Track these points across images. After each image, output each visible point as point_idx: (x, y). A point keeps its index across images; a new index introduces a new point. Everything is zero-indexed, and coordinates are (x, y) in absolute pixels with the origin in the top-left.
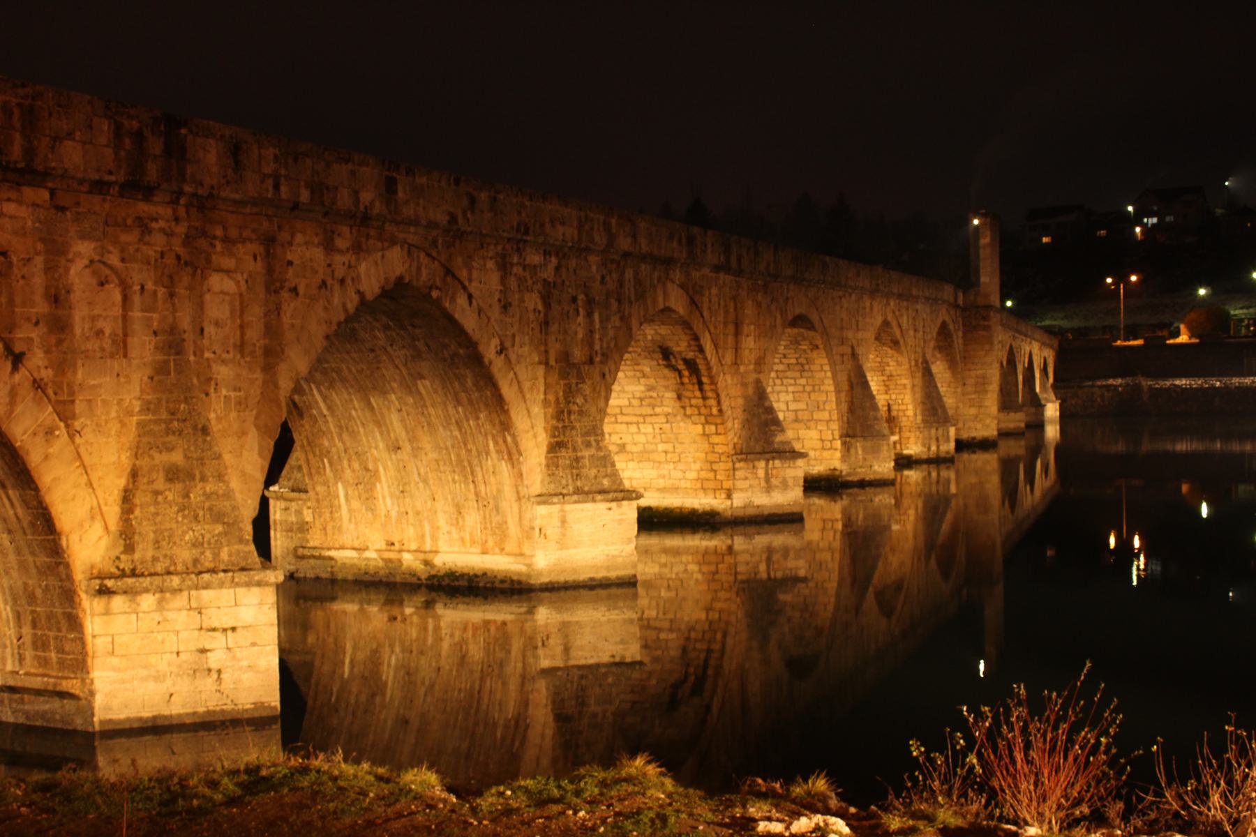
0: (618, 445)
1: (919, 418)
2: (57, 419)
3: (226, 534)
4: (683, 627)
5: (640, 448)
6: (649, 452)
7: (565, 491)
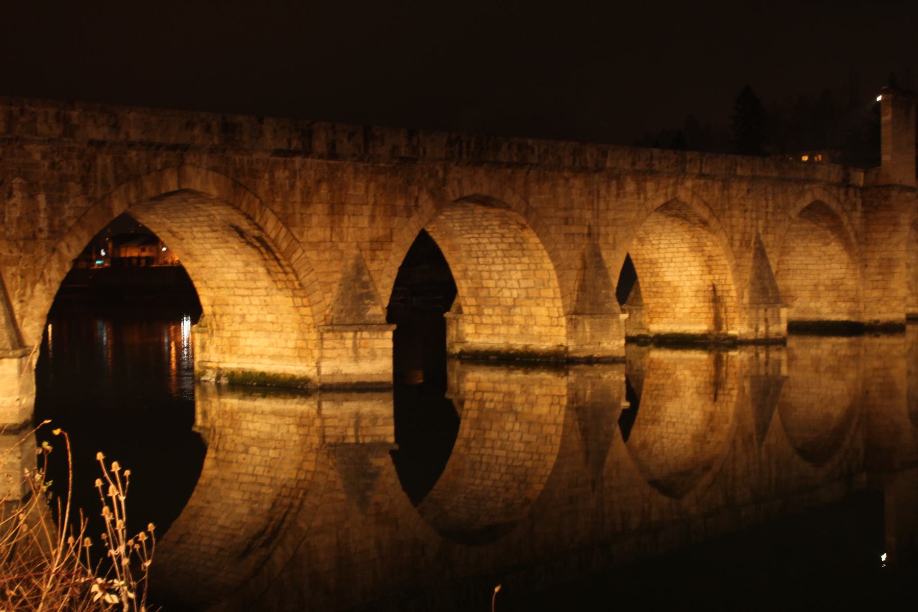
1: (746, 300)
4: (279, 483)
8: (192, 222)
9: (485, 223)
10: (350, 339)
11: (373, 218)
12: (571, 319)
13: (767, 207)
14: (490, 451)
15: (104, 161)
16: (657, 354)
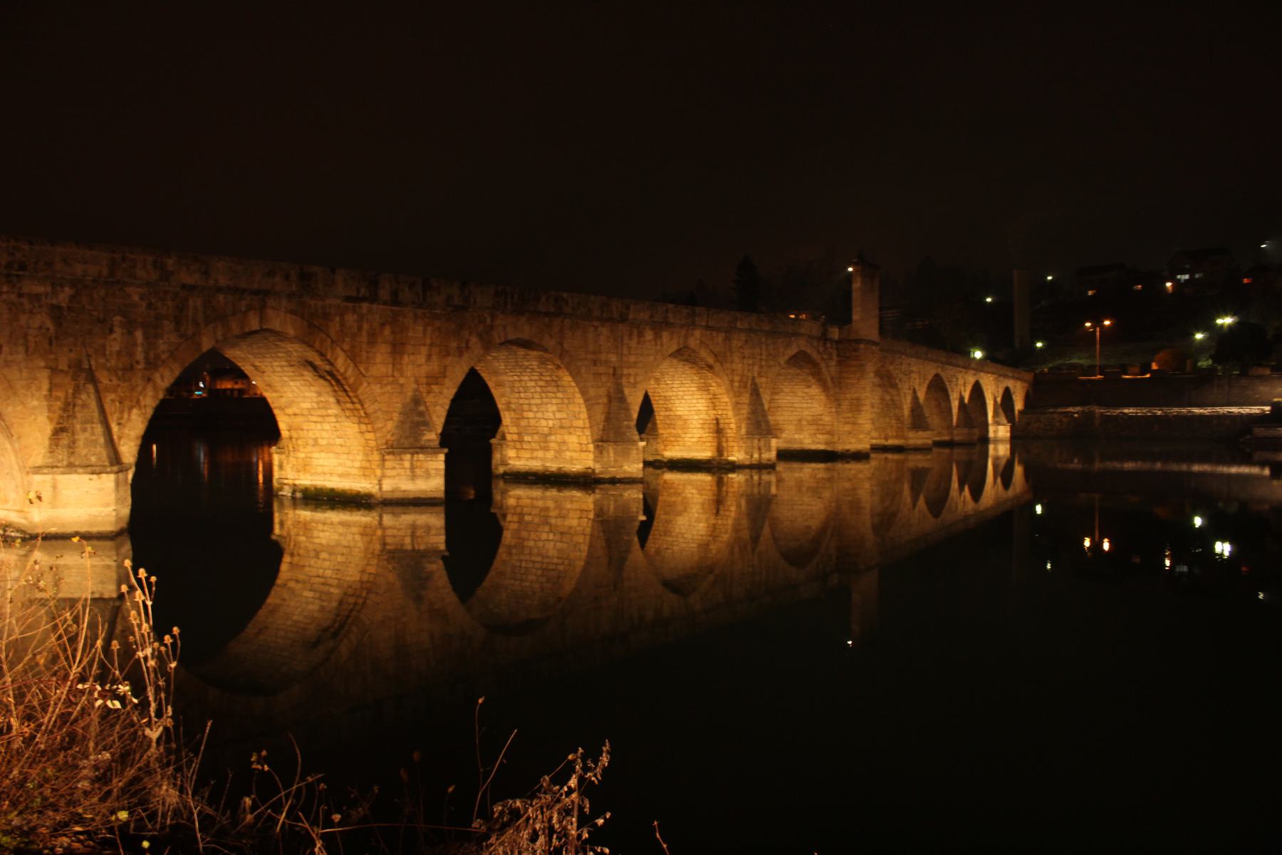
0: (313, 439)
1: (743, 431)
6: (332, 445)
8: (272, 357)
9: (526, 364)
10: (407, 460)
11: (429, 357)
12: (598, 446)
13: (761, 355)
14: (527, 557)
15: (195, 303)
16: (669, 476)
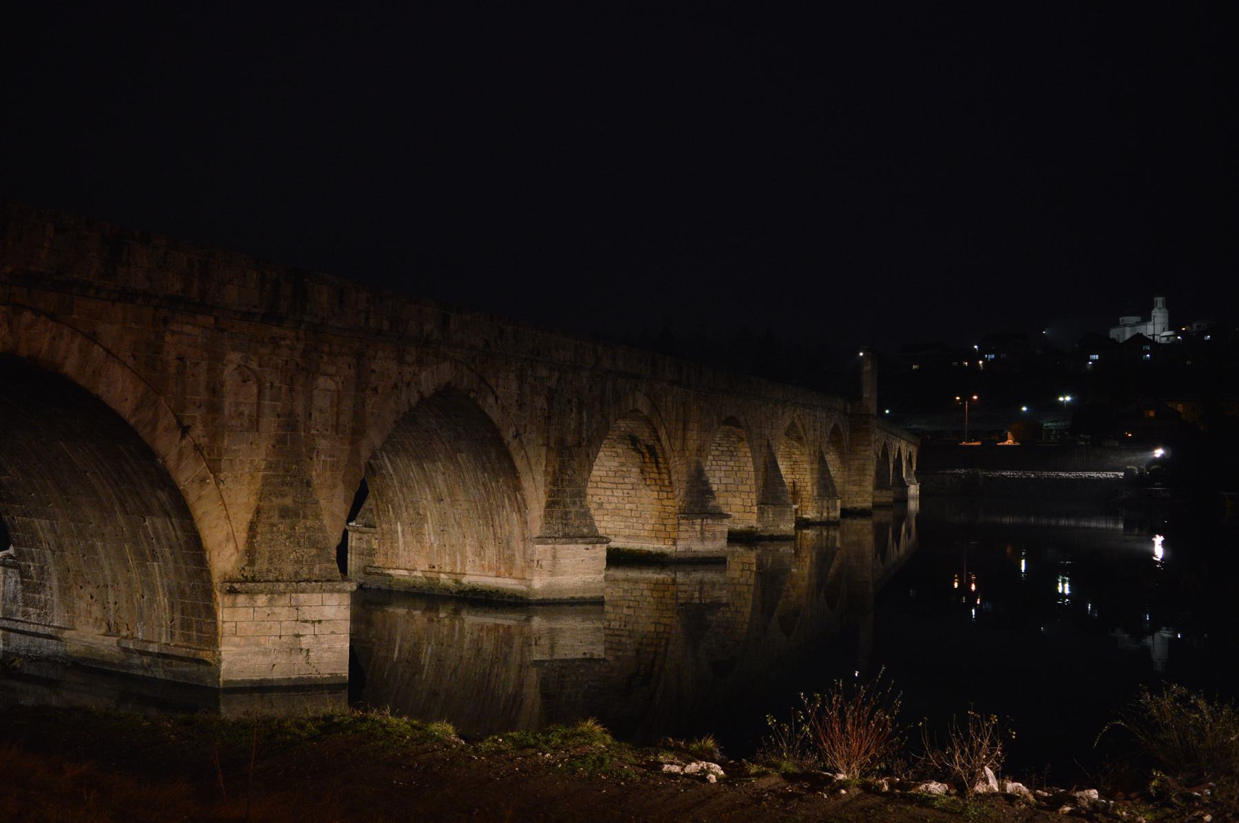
0: (598, 503)
1: (815, 493)
2: (208, 471)
3: (318, 555)
5: (613, 506)
6: (619, 510)
7: (556, 536)
12: (761, 508)
